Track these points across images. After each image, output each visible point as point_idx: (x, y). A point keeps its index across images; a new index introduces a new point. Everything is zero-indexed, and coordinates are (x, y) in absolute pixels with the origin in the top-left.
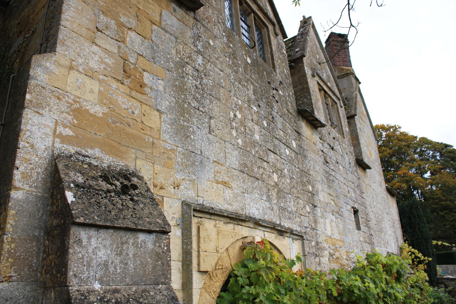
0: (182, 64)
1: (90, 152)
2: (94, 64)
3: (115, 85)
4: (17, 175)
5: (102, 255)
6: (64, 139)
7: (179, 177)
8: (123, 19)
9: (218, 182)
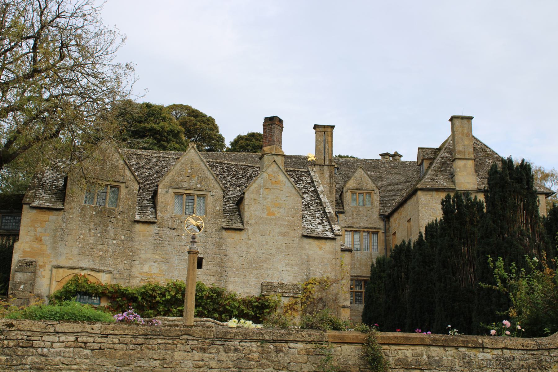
0: (56, 229)
1: (26, 258)
2: (27, 240)
3: (33, 243)
4: (12, 265)
5: (20, 276)
6: (21, 257)
7: (51, 260)
8: (36, 226)
9: (67, 259)
